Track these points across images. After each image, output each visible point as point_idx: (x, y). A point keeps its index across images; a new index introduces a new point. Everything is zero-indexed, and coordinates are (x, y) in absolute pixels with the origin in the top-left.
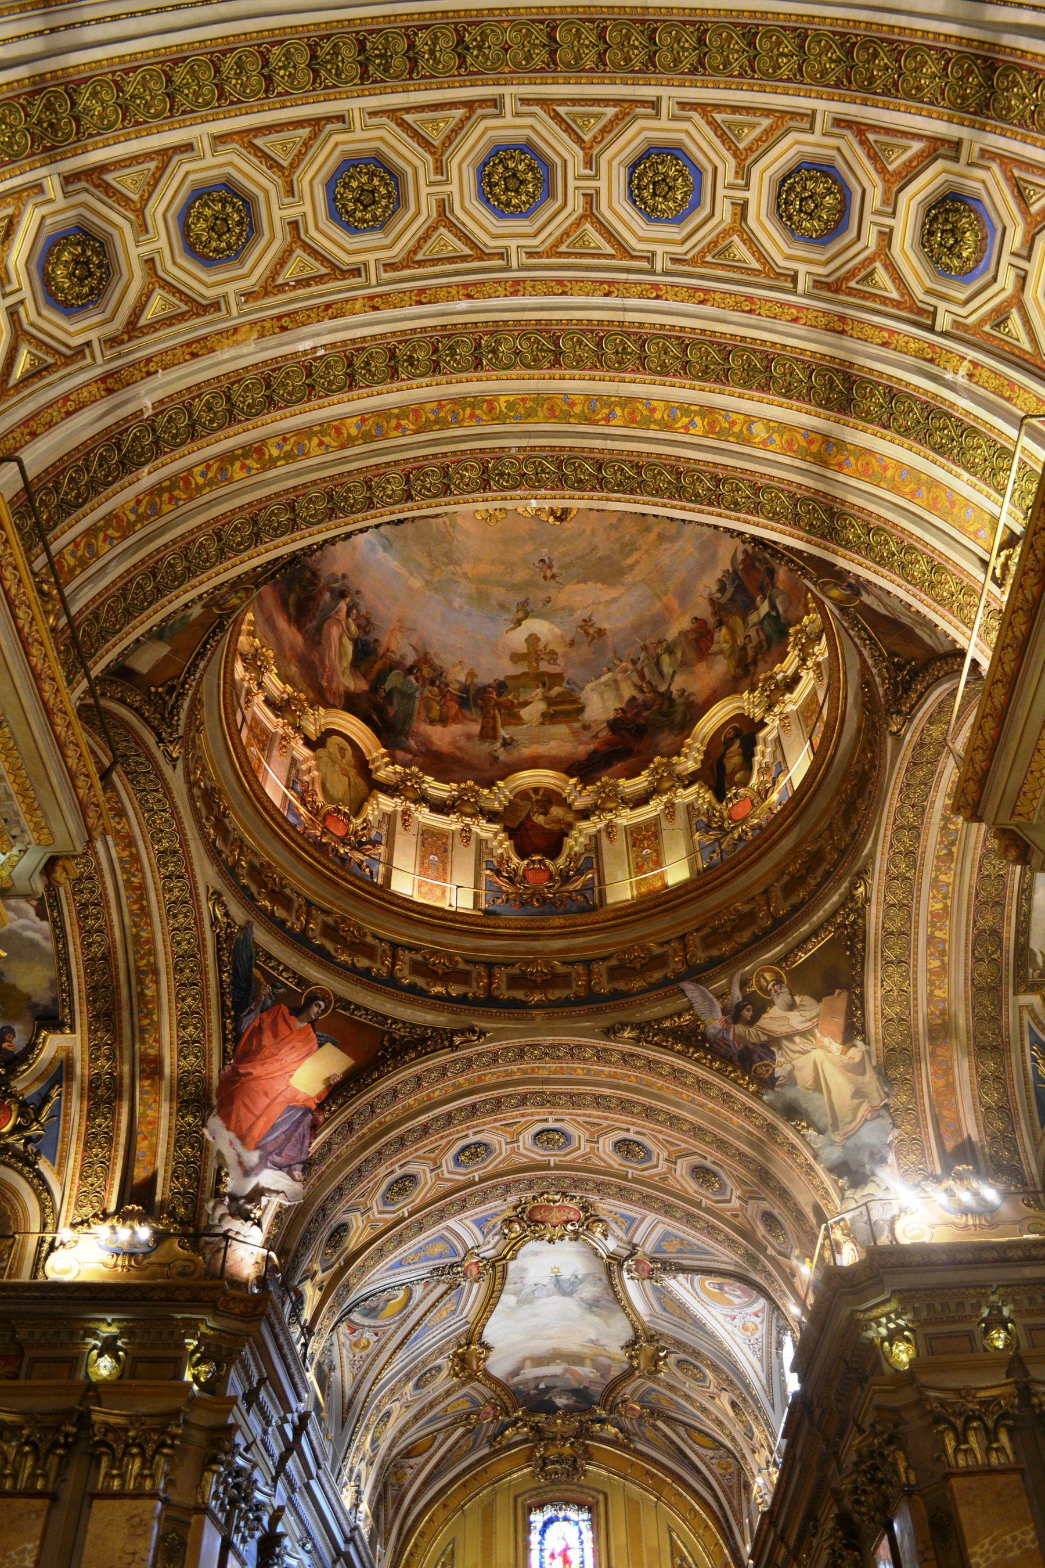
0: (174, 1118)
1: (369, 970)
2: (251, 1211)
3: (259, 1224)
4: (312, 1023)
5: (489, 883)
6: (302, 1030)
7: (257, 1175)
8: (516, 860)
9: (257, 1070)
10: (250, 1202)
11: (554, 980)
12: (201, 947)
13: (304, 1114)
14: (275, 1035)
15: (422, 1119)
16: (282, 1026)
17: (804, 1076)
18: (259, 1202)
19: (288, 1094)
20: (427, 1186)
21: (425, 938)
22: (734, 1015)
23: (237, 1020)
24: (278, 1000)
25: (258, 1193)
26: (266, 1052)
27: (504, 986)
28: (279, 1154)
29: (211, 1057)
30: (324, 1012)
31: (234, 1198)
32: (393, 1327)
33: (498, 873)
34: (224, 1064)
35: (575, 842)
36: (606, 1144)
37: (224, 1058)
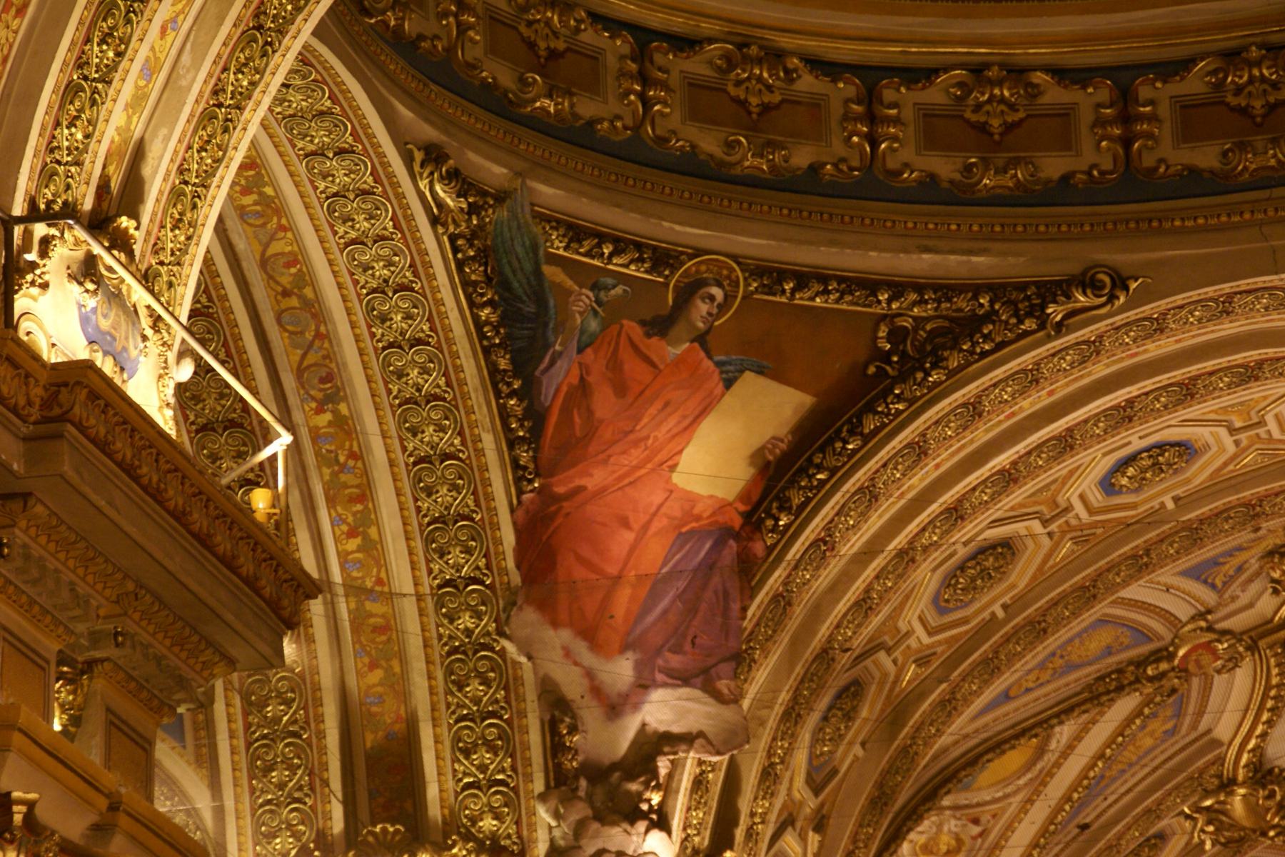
0: (432, 619)
1: (815, 169)
2: (639, 797)
3: (662, 823)
4: (701, 339)
6: (679, 361)
7: (637, 707)
9: (596, 478)
10: (632, 777)
12: (420, 266)
13: (719, 544)
14: (621, 389)
15: (1002, 460)
16: (634, 368)
18: (654, 773)
19: (674, 508)
23: (528, 392)
24: (611, 313)
26: (607, 434)
27: (1165, 132)
28: (677, 650)
29: (487, 483)
30: (723, 308)
31: (597, 773)
32: (1016, 801)
34: (520, 492)
37: (518, 480)
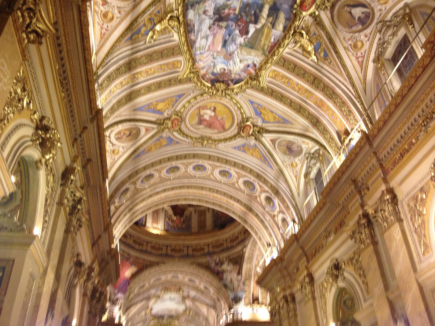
5: (167, 222)
8: (173, 217)
11: (180, 251)
17: (229, 279)
20: (147, 285)
21: (154, 240)
22: (217, 264)
25: (117, 299)
33: (169, 219)
35: (187, 213)
36: (186, 280)
